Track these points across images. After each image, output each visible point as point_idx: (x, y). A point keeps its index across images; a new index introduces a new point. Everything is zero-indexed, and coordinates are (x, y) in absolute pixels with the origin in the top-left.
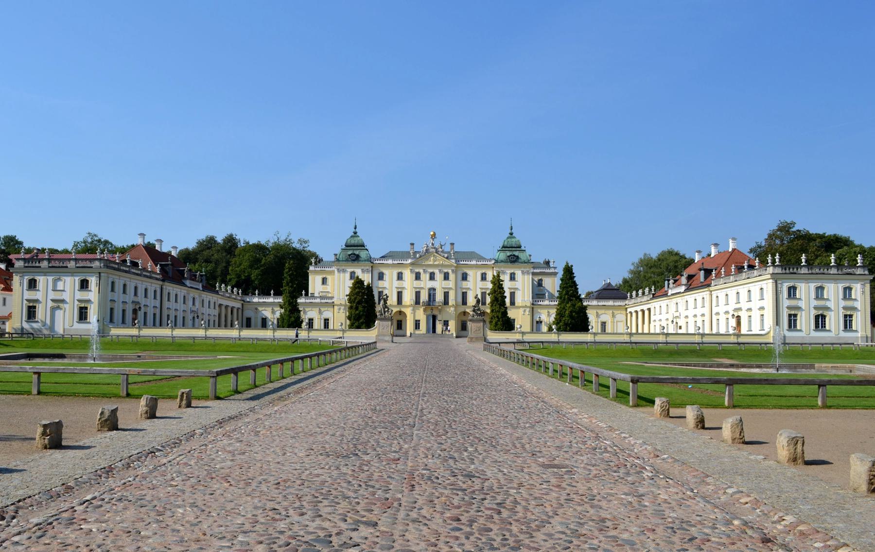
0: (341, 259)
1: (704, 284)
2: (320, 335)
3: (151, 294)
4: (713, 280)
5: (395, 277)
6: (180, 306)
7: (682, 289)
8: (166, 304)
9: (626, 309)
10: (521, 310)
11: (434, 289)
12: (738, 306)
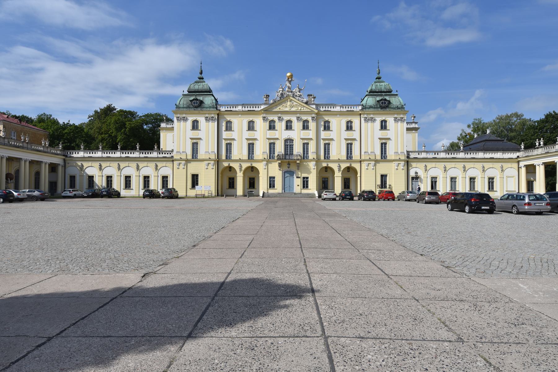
0: (182, 106)
5: (246, 126)
9: (518, 162)
10: (394, 165)
11: (291, 140)
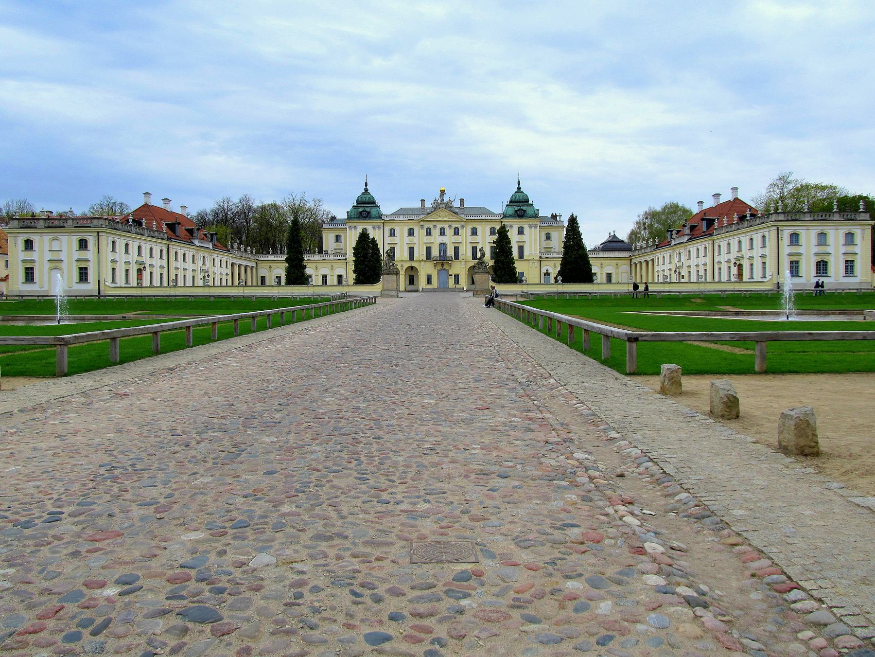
1: (706, 233)
2: (333, 290)
3: (155, 252)
4: (715, 229)
5: (406, 233)
6: (189, 265)
7: (686, 238)
8: (173, 264)
9: (631, 260)
11: (445, 245)
12: (740, 254)
